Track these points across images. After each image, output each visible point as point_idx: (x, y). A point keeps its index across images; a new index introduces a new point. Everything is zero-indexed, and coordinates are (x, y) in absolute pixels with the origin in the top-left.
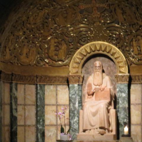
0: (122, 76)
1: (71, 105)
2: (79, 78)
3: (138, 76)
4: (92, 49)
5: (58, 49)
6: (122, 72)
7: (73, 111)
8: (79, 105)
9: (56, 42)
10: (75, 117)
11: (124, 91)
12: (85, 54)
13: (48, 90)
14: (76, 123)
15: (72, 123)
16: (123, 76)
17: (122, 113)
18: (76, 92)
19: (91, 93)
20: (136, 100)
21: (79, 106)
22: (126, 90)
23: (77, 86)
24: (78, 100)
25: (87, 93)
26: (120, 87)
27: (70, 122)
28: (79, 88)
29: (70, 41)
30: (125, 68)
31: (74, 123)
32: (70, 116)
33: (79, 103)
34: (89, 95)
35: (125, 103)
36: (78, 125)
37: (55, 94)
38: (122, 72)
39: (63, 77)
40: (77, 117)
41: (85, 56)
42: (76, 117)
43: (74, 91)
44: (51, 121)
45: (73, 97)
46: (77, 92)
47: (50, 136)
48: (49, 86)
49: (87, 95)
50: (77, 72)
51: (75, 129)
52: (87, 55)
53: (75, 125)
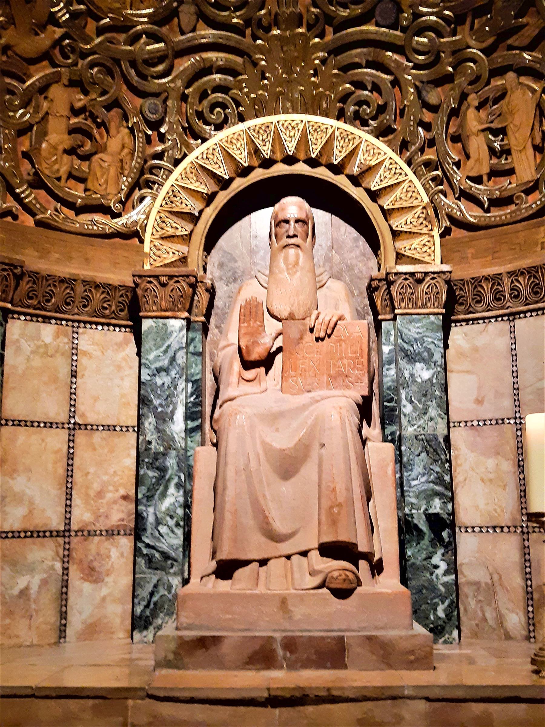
0: (412, 274)
1: (150, 423)
2: (193, 286)
3: (496, 279)
4: (257, 151)
5: (88, 146)
6: (414, 261)
7: (156, 456)
8: (191, 424)
9: (78, 105)
10: (166, 488)
11: (425, 354)
12: (223, 172)
13: (27, 347)
14: (172, 523)
15: (151, 519)
16: (420, 276)
17: (418, 469)
18: (173, 359)
19: (256, 354)
20: (479, 401)
21: (189, 432)
22: (432, 347)
23: (181, 330)
24: (183, 397)
25: (240, 349)
26: (405, 331)
27: (139, 518)
28: (193, 340)
29: (152, 117)
30: (426, 238)
31: (158, 522)
32: (139, 480)
33: (190, 416)
34: (247, 365)
35: (433, 412)
36: (179, 532)
37: (64, 371)
38: (414, 261)
39: (108, 288)
40: (179, 486)
41: (224, 184)
42: (172, 490)
43: (166, 351)
44: (31, 512)
45: (159, 381)
46: (181, 358)
47: (24, 593)
48: (33, 326)
49: (237, 365)
50: (184, 260)
51: (166, 556)
52: (231, 180)
53: (163, 529)
